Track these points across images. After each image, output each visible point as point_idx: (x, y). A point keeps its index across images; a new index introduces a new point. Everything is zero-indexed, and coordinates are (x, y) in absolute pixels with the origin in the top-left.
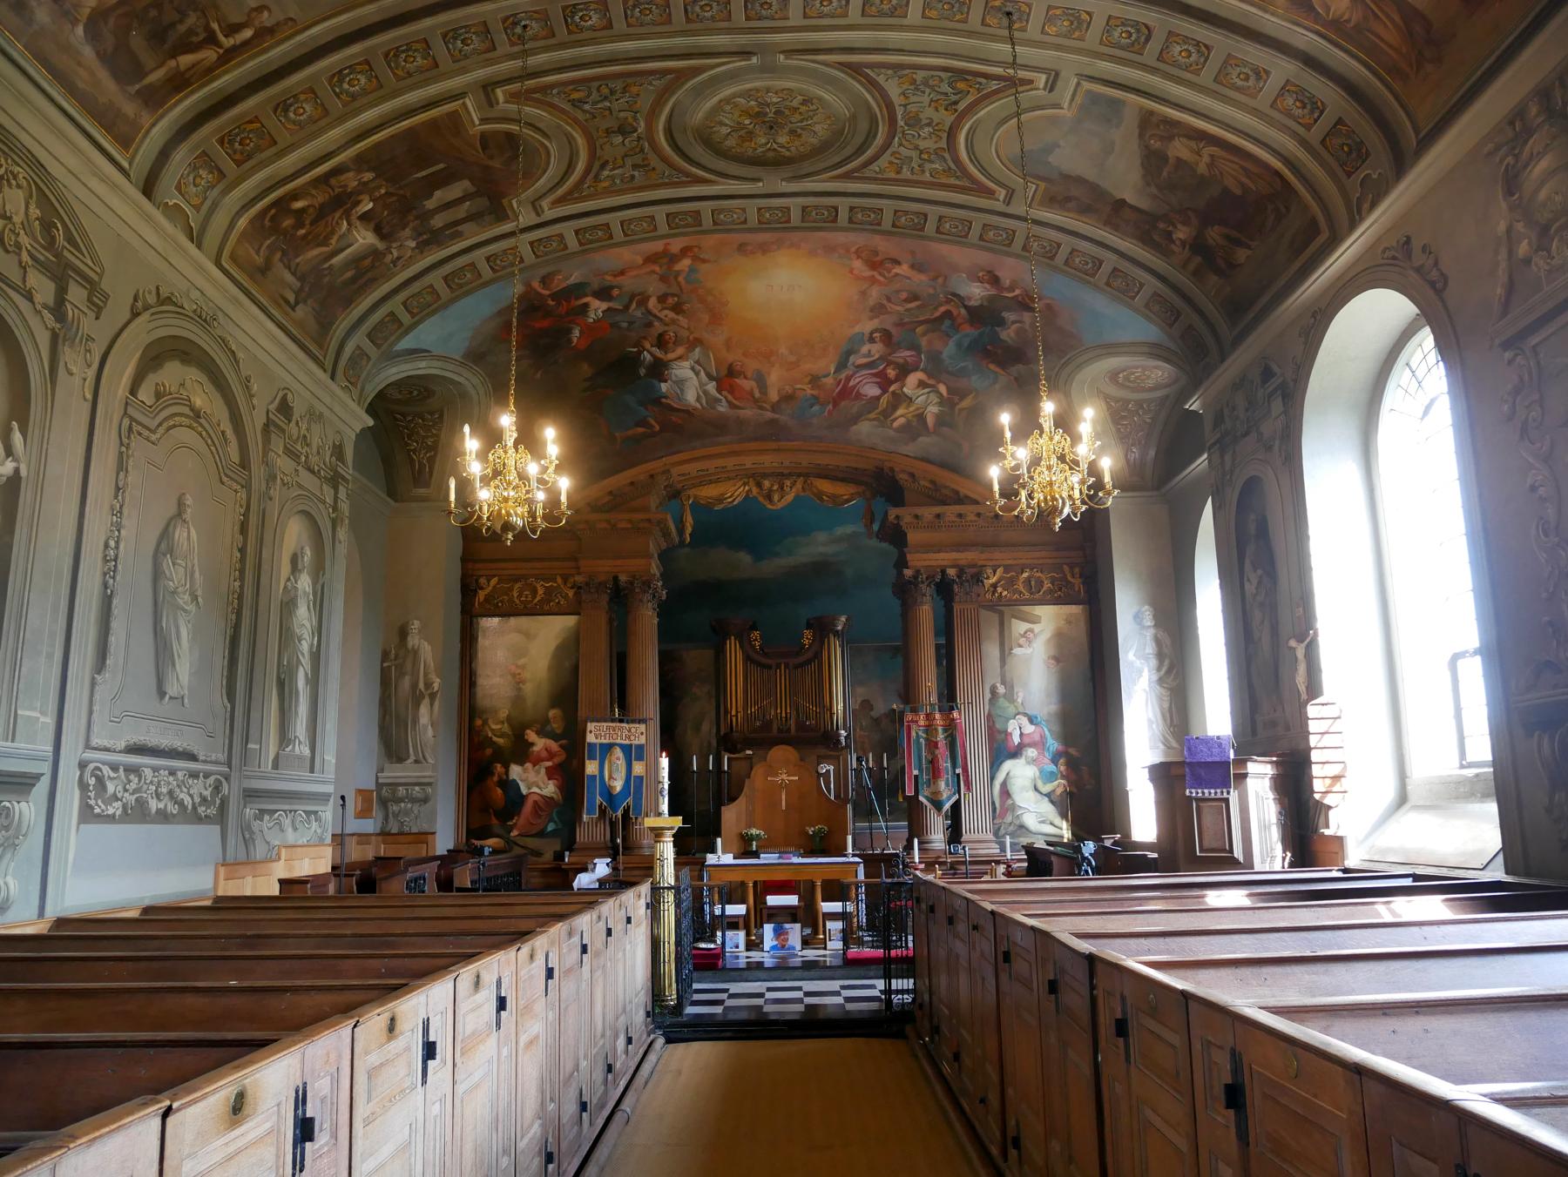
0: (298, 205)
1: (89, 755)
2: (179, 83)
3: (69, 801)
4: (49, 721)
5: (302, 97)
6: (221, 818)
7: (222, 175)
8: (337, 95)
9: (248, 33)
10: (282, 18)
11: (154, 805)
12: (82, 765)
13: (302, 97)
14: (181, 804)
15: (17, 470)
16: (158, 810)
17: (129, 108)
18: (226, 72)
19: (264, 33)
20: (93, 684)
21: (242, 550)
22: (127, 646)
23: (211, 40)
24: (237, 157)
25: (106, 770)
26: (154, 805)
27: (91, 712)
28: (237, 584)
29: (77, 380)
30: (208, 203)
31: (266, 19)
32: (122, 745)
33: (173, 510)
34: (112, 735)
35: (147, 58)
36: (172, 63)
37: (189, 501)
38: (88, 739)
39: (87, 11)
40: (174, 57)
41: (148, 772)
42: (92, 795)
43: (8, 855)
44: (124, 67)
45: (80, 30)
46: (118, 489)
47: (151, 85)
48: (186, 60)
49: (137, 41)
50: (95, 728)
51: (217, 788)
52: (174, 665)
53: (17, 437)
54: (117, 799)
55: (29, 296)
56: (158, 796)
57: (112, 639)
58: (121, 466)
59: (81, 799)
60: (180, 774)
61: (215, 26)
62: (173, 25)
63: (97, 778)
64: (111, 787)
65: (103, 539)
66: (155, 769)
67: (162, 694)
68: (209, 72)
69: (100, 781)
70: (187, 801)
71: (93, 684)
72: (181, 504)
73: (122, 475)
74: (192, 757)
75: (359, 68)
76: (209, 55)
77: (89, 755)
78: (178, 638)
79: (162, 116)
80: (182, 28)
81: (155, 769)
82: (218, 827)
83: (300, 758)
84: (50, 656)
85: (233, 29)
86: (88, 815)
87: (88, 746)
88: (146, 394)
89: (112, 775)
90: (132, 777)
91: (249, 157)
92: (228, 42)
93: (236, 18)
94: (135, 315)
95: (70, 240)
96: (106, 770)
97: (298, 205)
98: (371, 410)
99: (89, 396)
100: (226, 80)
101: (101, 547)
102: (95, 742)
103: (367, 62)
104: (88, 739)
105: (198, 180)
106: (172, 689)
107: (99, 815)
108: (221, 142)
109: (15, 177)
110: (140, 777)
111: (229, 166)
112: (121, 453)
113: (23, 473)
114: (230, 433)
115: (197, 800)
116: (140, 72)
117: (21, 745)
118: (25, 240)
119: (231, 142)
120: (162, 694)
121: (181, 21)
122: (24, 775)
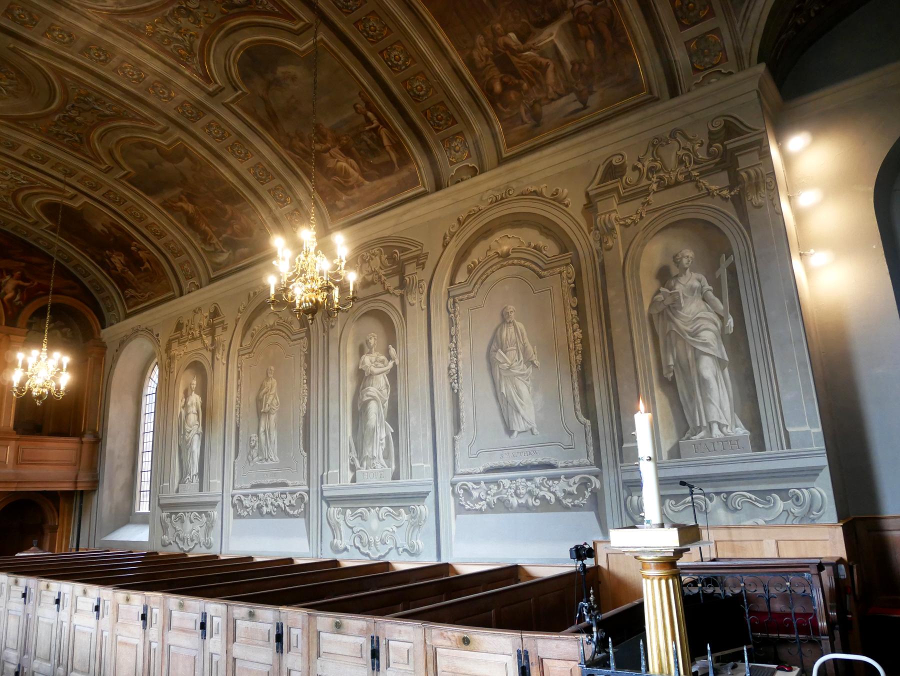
0: (498, 87)
1: (456, 478)
2: (399, 147)
3: (448, 504)
4: (429, 465)
5: (409, 87)
7: (460, 133)
8: (407, 67)
9: (370, 114)
10: (360, 99)
12: (453, 485)
13: (409, 87)
14: (543, 498)
15: (394, 364)
16: (519, 505)
17: (405, 173)
18: (393, 125)
19: (369, 106)
20: (454, 441)
22: (475, 414)
23: (375, 130)
24: (450, 123)
25: (470, 485)
26: (515, 501)
27: (454, 456)
28: (578, 333)
29: (417, 305)
30: (472, 148)
31: (361, 106)
32: (482, 469)
33: (497, 320)
34: (472, 464)
35: (385, 158)
36: (388, 148)
37: (511, 308)
38: (454, 469)
39: (360, 178)
40: (384, 147)
41: (507, 483)
42: (463, 499)
43: (417, 530)
44: (386, 169)
45: (367, 183)
46: (451, 336)
47: (397, 160)
48: (386, 142)
49: (375, 161)
50: (459, 464)
51: (585, 483)
52: (518, 412)
53: (392, 351)
54: (482, 500)
55: (387, 292)
56: (517, 495)
59: (455, 502)
60: (538, 480)
61: (367, 128)
62: (368, 145)
63: (465, 490)
64: (475, 494)
65: (447, 366)
66: (512, 479)
67: (509, 432)
68: (393, 132)
69: (467, 492)
70: (549, 496)
71: (454, 441)
73: (453, 329)
75: (386, 56)
76: (383, 132)
77: (456, 478)
78: (519, 394)
79: (415, 160)
80: (369, 142)
81: (512, 479)
82: (592, 515)
83: (737, 439)
84: (425, 435)
85: (369, 121)
86: (460, 509)
87: (455, 474)
88: (461, 277)
89: (475, 486)
90: (492, 486)
91: (452, 116)
92: (376, 123)
93: (362, 119)
94: (445, 246)
96: (470, 485)
97: (498, 87)
99: (424, 307)
100: (398, 124)
101: (446, 370)
102: (459, 471)
103: (381, 53)
104: (454, 469)
105: (457, 148)
107: (469, 510)
108: (437, 131)
109: (373, 254)
110: (499, 486)
111: (456, 128)
112: (451, 319)
113: (397, 362)
115: (560, 495)
116: (390, 163)
117: (415, 480)
118: (382, 272)
119: (439, 125)
120: (509, 432)
121: (366, 142)
122: (419, 493)
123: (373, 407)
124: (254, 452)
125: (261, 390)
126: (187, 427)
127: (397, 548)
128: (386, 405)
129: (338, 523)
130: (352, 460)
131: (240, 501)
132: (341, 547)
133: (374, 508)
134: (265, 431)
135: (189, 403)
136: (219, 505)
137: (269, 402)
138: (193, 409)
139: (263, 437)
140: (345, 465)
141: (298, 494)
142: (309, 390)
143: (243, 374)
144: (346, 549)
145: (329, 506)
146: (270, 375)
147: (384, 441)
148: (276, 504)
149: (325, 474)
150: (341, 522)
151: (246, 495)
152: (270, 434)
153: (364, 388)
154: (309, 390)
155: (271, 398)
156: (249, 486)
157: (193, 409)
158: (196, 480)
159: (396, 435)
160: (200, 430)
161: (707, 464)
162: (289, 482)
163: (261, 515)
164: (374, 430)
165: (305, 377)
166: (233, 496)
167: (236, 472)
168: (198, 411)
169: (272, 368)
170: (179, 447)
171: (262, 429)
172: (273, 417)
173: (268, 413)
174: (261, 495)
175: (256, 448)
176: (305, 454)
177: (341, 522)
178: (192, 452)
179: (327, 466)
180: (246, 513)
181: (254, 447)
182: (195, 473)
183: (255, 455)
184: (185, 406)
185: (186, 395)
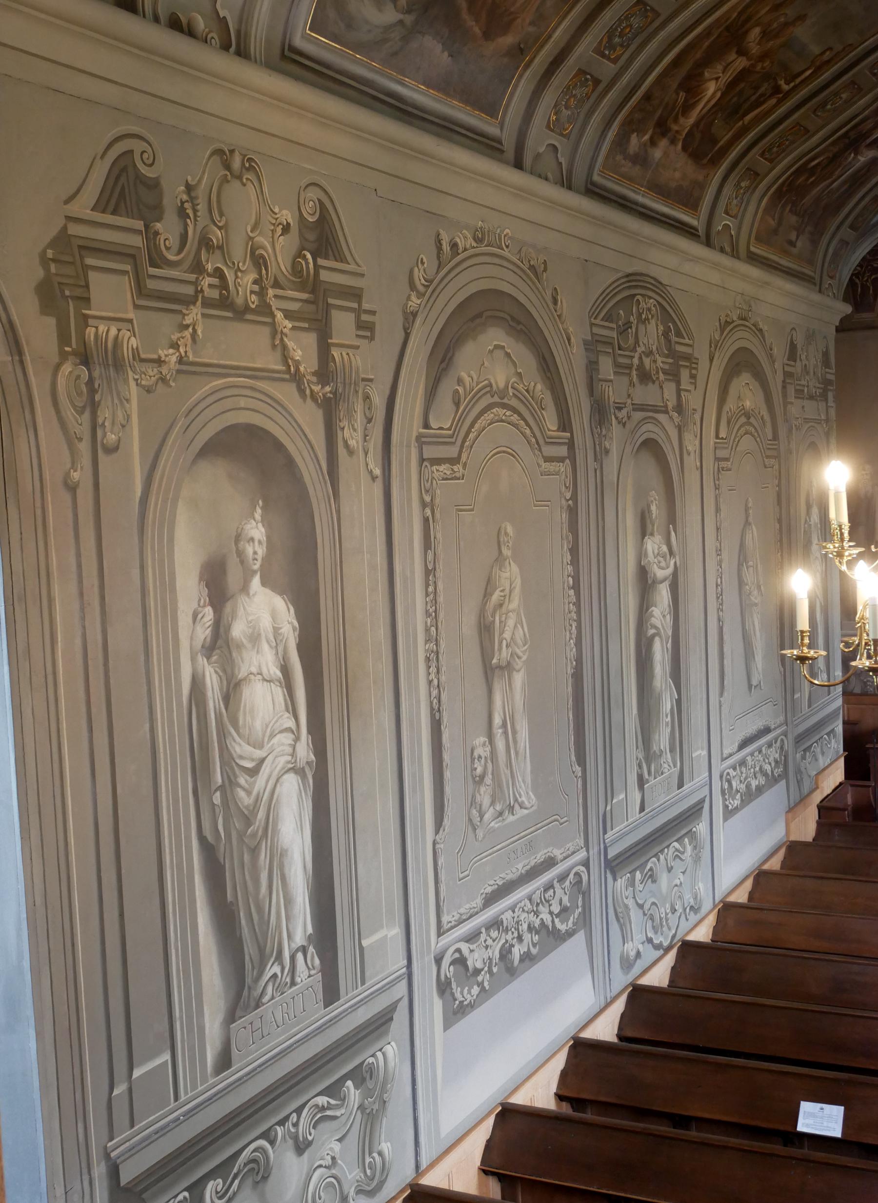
6: (785, 775)
11: (754, 783)
21: (780, 521)
46: (718, 529)
57: (725, 662)
58: (718, 510)
72: (747, 509)
74: (767, 730)
81: (752, 754)
94: (711, 360)
95: (679, 334)
98: (845, 300)
106: (754, 682)
114: (767, 417)
123: (657, 646)
124: (484, 797)
125: (487, 595)
126: (240, 748)
127: (685, 910)
128: (669, 645)
129: (626, 907)
130: (640, 766)
131: (460, 961)
132: (633, 954)
133: (662, 851)
134: (504, 725)
135: (238, 630)
136: (401, 1016)
137: (507, 635)
138: (260, 661)
139: (500, 744)
140: (633, 779)
141: (571, 876)
142: (578, 604)
143: (438, 533)
144: (638, 954)
145: (615, 880)
146: (506, 552)
147: (669, 719)
148: (537, 923)
149: (609, 808)
150: (630, 902)
151: (472, 938)
152: (514, 732)
153: (647, 610)
154: (578, 604)
155: (511, 623)
156: (479, 902)
157: (260, 661)
158: (307, 971)
159: (679, 702)
160: (305, 752)
161: (822, 709)
162: (558, 853)
163: (512, 972)
164: (659, 698)
165: (570, 568)
166: (438, 961)
167: (443, 876)
168: (285, 670)
169: (510, 530)
170: (209, 850)
171: (497, 720)
172: (519, 678)
173: (508, 668)
174: (507, 917)
175: (488, 780)
176: (578, 770)
177: (630, 902)
178: (279, 857)
179: (610, 792)
180: (476, 990)
181: (482, 777)
182: (299, 939)
183: (486, 801)
184: (219, 643)
185: (218, 587)
